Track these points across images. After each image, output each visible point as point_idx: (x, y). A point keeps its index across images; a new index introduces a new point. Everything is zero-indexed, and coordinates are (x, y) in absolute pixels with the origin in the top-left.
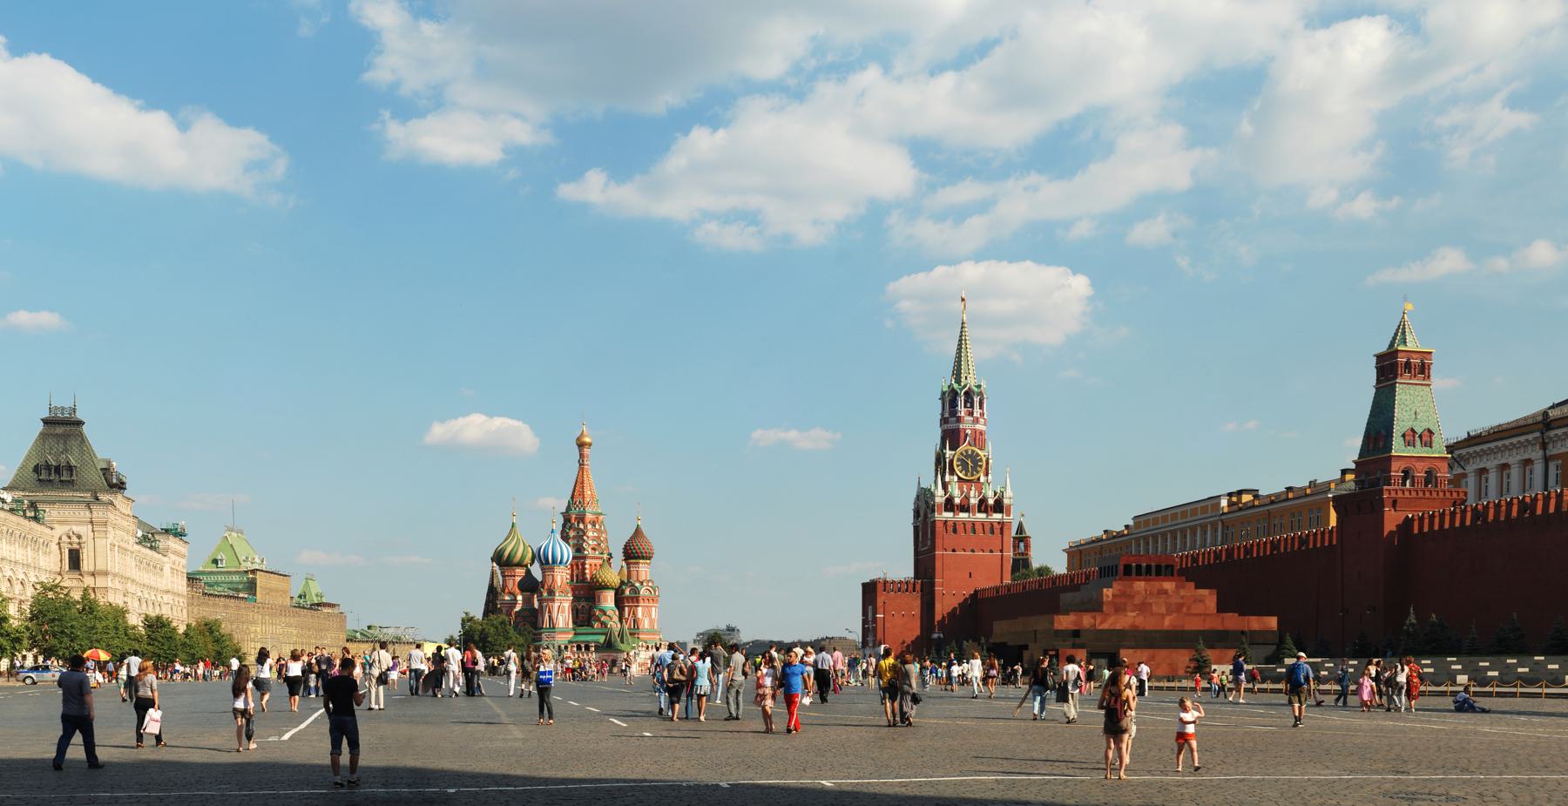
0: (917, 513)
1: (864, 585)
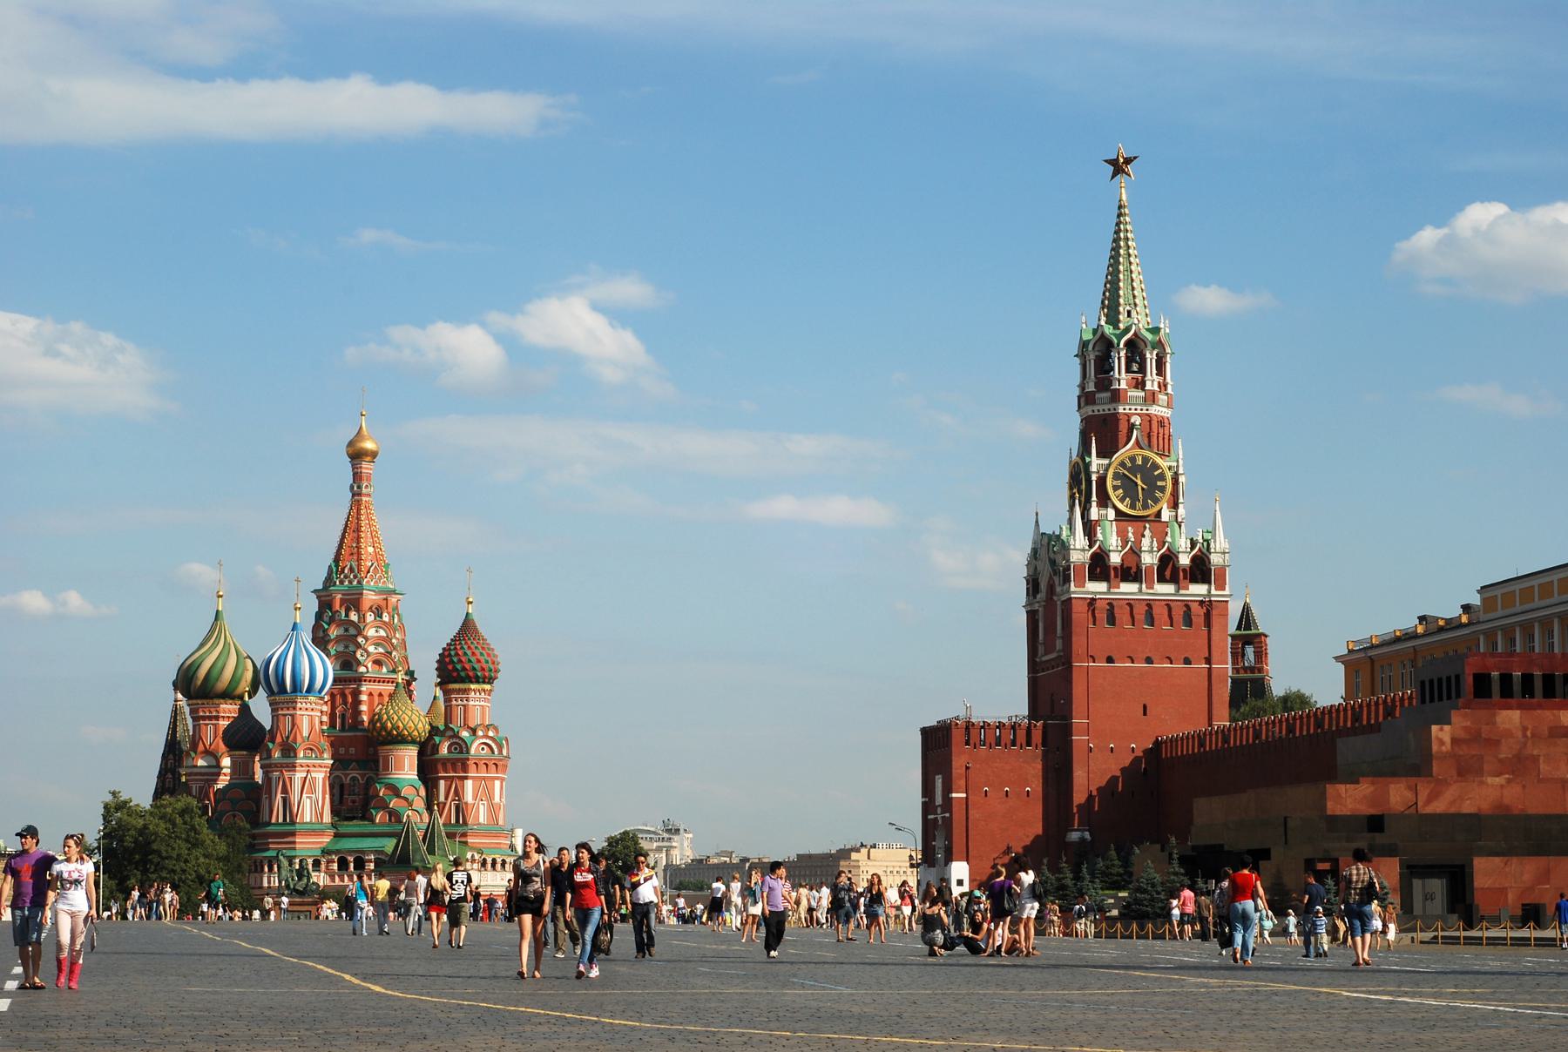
0: (1033, 585)
1: (926, 732)
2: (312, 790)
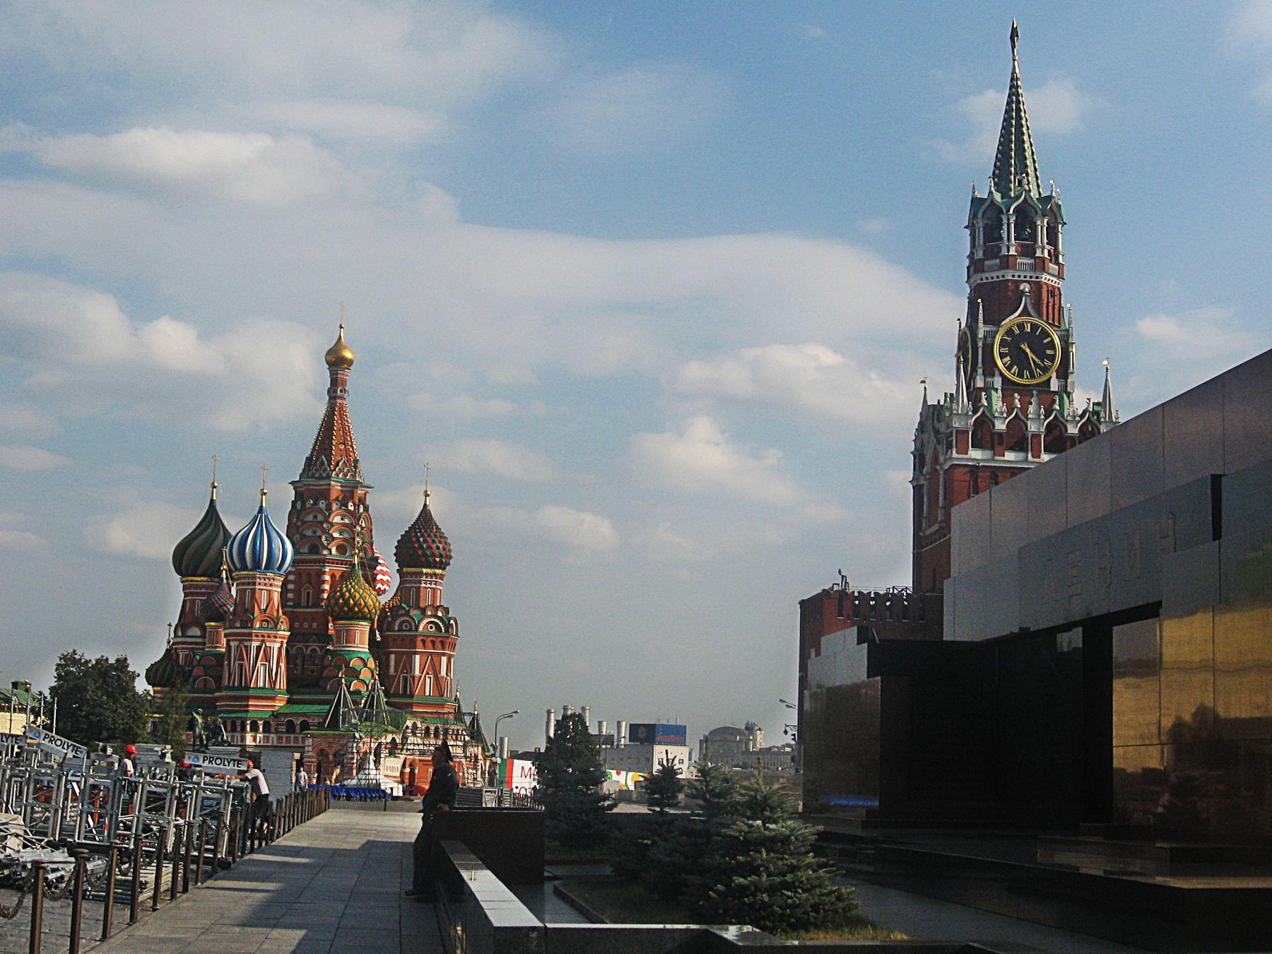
2: (267, 659)
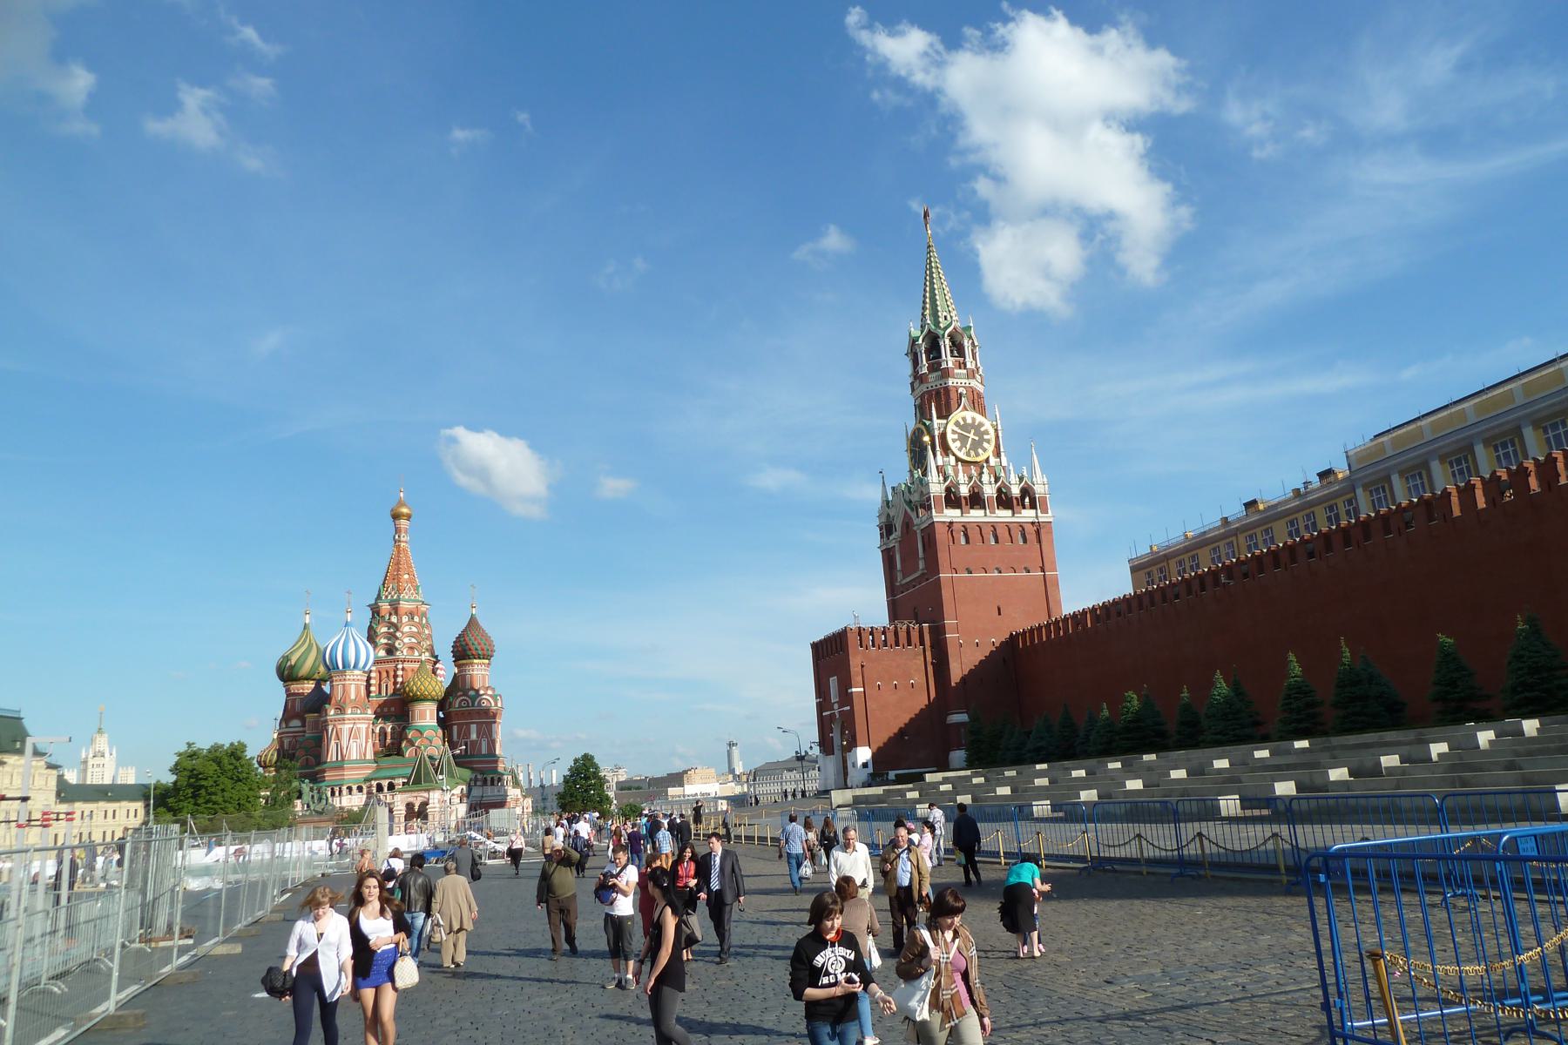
0: (887, 529)
1: (816, 647)
